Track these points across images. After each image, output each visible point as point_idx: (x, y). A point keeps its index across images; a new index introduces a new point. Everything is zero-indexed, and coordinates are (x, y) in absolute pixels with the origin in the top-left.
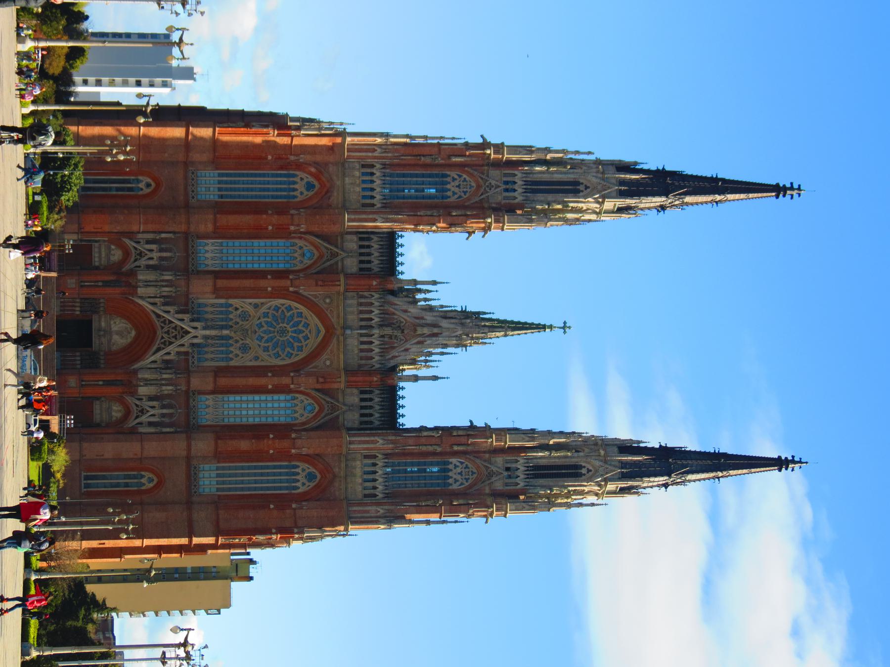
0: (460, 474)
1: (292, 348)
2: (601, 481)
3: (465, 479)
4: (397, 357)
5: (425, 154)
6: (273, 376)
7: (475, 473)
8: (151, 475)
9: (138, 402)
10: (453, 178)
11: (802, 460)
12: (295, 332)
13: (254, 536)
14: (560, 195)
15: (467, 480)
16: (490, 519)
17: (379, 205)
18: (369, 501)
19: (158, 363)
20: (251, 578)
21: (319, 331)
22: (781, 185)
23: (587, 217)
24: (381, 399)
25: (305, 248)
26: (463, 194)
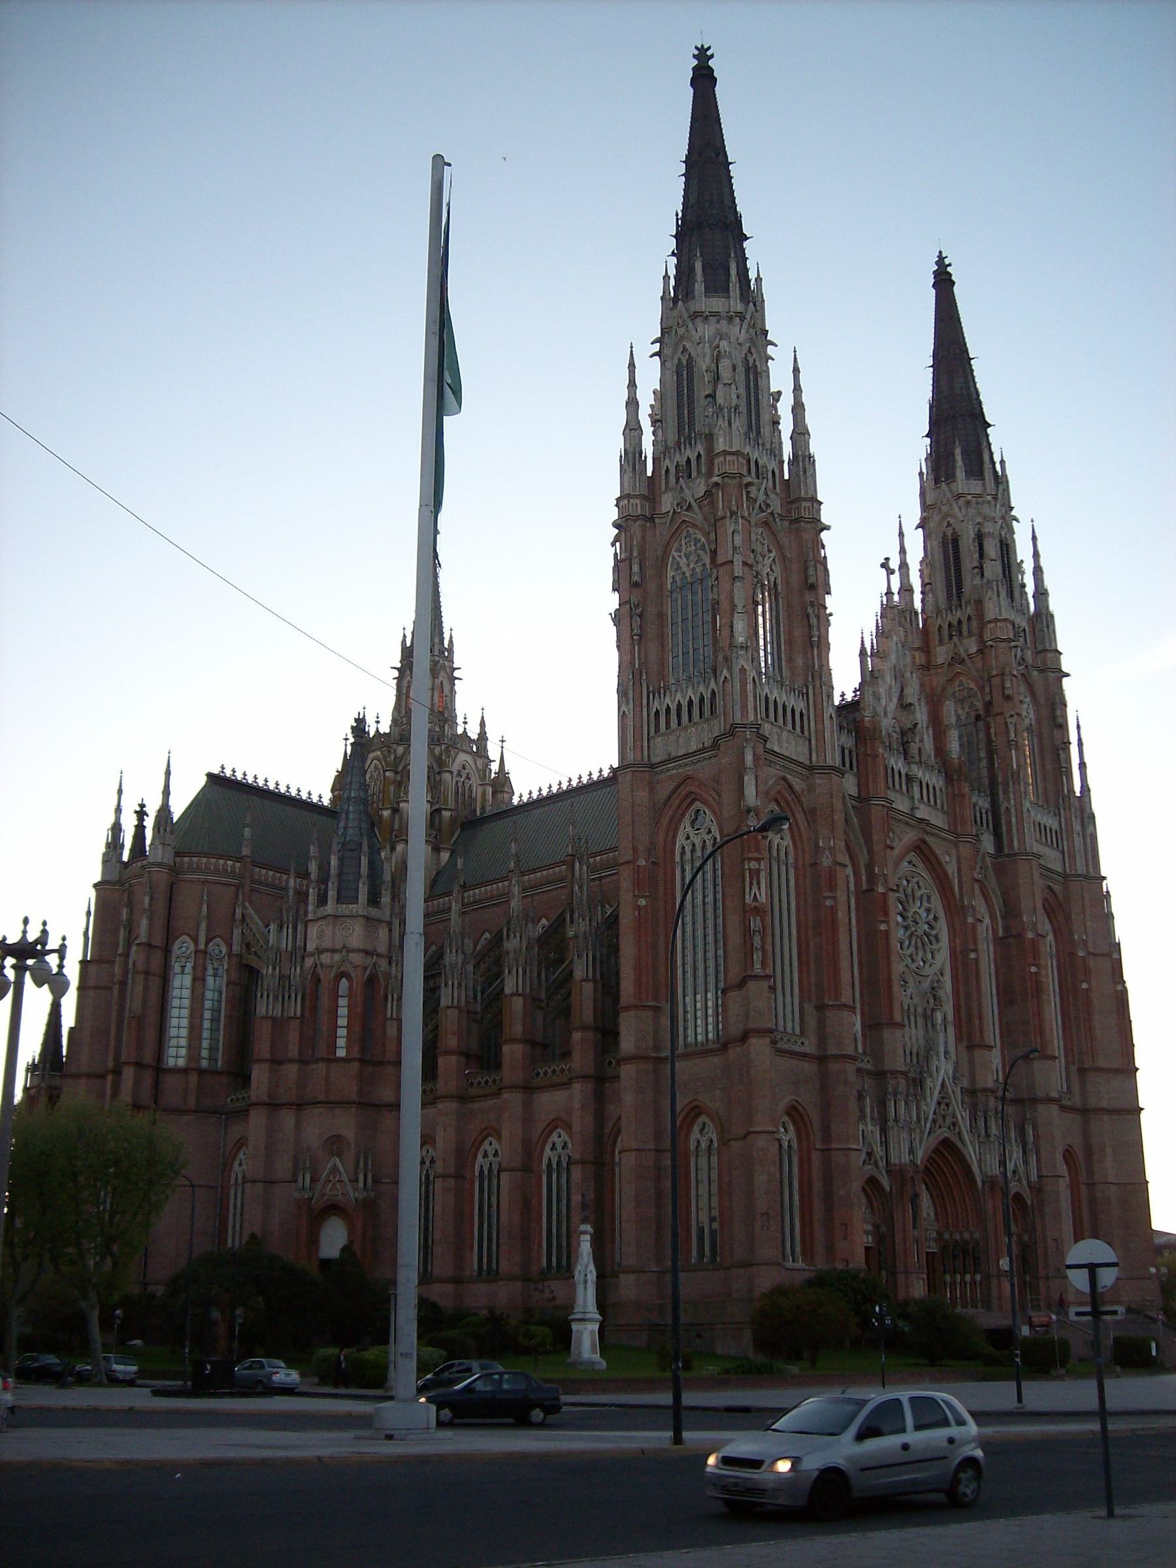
6: (976, 950)
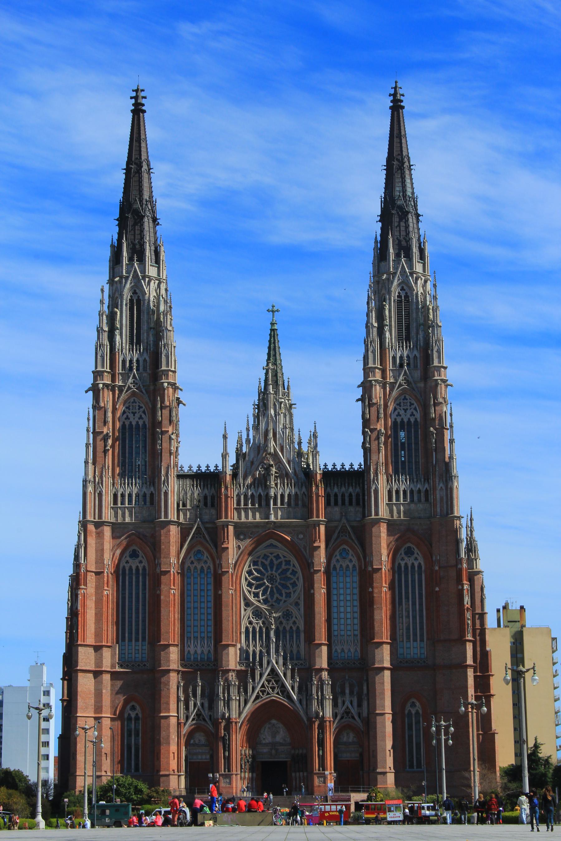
0: (405, 410)
1: (287, 570)
2: (412, 278)
3: (410, 406)
5: (103, 446)
7: (405, 397)
8: (409, 704)
9: (338, 718)
10: (126, 419)
11: (394, 86)
12: (272, 568)
13: (464, 605)
14: (142, 317)
15: (411, 404)
16: (448, 383)
17: (152, 489)
18: (432, 496)
19: (301, 698)
20: (522, 608)
21: (271, 545)
22: (133, 108)
23: (163, 292)
24: (336, 486)
25: (192, 559)
26: (142, 410)
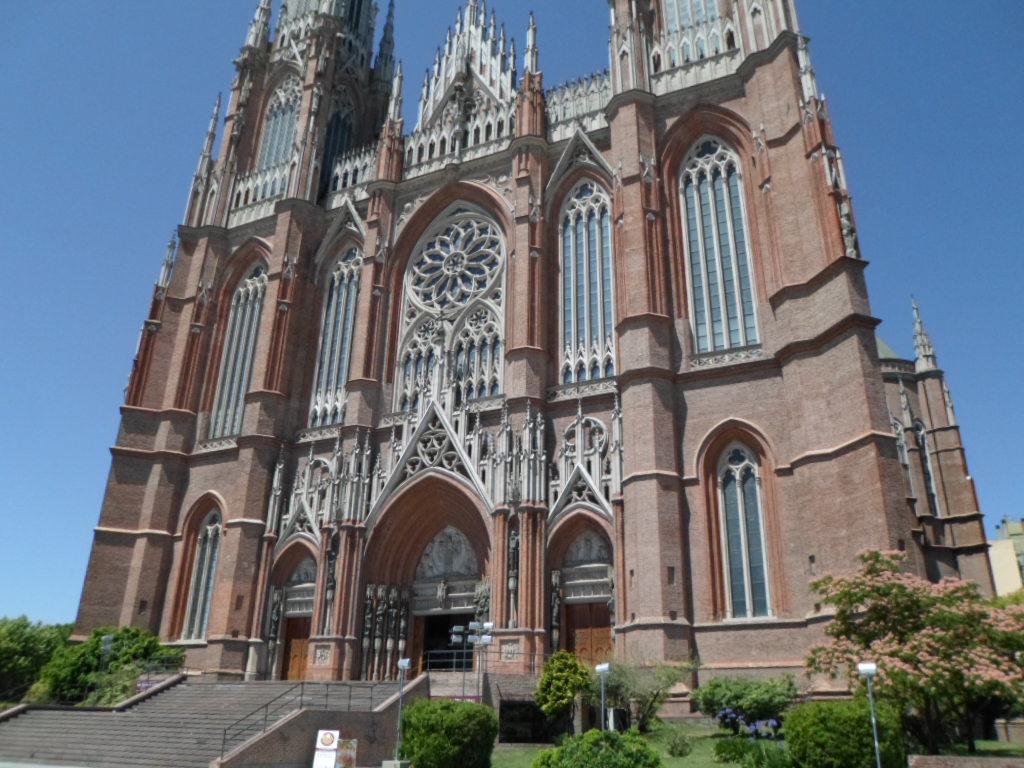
4: (501, 90)
8: (725, 456)
